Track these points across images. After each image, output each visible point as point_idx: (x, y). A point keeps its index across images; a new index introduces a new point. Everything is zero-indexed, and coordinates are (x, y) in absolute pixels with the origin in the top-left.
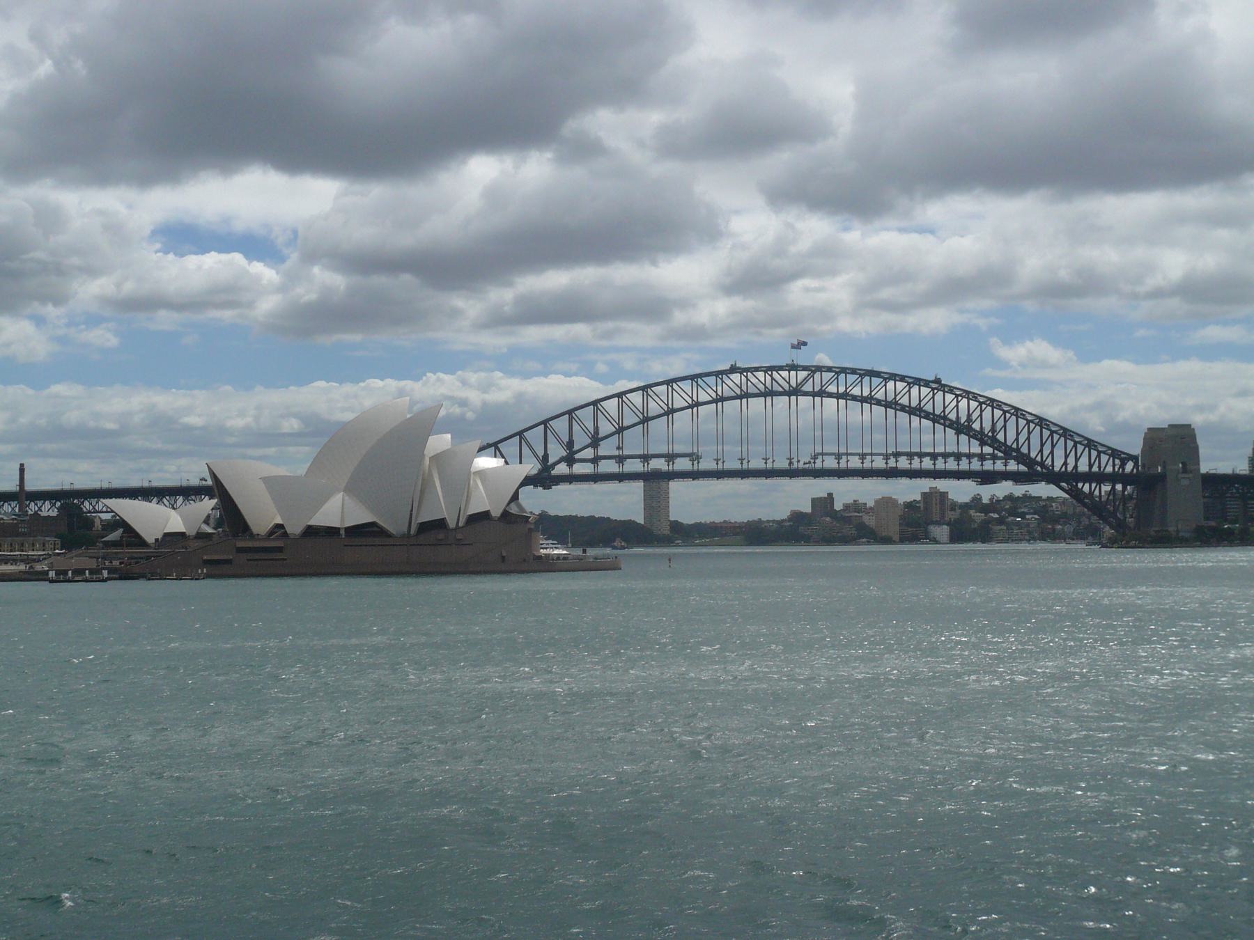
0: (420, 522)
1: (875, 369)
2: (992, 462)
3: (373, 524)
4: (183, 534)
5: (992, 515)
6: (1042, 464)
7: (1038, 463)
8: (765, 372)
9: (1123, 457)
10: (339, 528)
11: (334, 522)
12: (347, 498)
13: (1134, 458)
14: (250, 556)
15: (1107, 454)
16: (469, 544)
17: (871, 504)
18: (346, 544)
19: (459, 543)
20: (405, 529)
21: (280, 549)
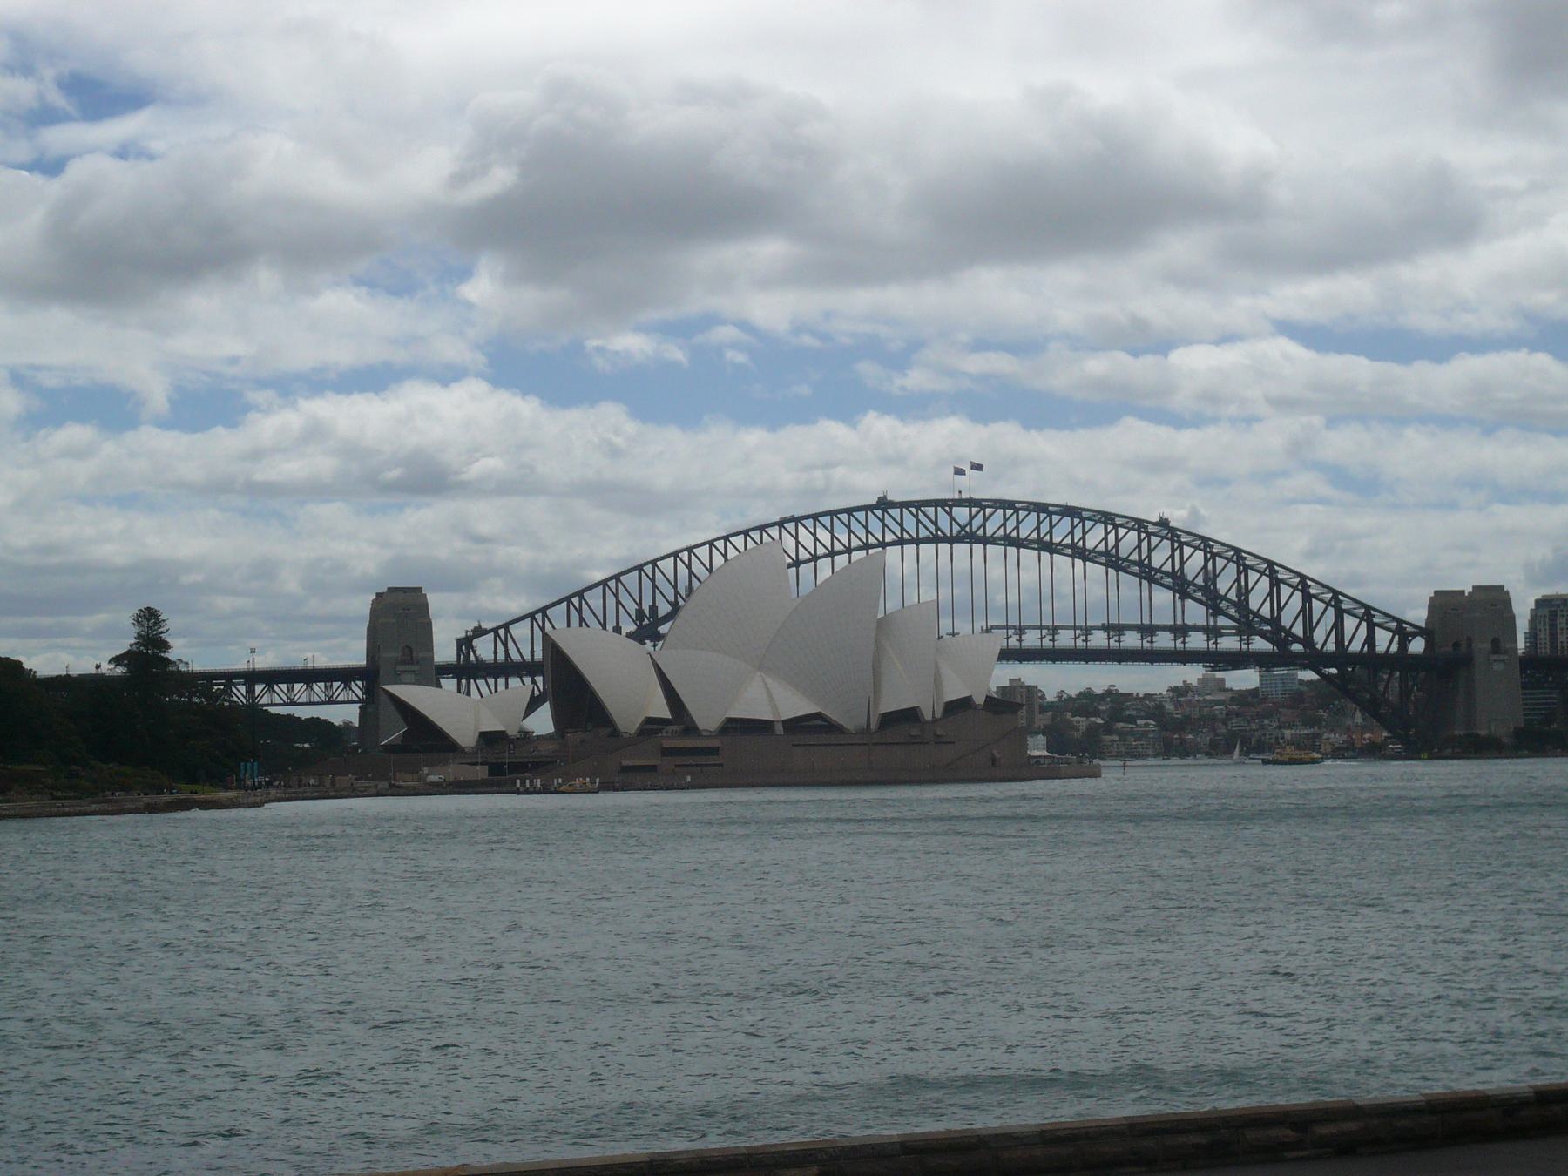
0: (884, 712)
1: (1069, 504)
2: (1238, 638)
3: (818, 716)
4: (503, 732)
5: (1093, 719)
6: (1307, 641)
7: (1296, 639)
8: (918, 508)
9: (1403, 631)
10: (773, 722)
11: (765, 714)
12: (768, 680)
13: (1420, 632)
14: (679, 760)
15: (1388, 629)
16: (950, 743)
17: (1051, 697)
18: (795, 743)
19: (938, 741)
20: (864, 722)
21: (714, 751)
